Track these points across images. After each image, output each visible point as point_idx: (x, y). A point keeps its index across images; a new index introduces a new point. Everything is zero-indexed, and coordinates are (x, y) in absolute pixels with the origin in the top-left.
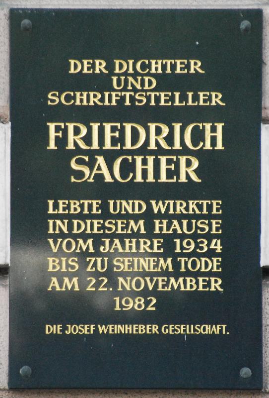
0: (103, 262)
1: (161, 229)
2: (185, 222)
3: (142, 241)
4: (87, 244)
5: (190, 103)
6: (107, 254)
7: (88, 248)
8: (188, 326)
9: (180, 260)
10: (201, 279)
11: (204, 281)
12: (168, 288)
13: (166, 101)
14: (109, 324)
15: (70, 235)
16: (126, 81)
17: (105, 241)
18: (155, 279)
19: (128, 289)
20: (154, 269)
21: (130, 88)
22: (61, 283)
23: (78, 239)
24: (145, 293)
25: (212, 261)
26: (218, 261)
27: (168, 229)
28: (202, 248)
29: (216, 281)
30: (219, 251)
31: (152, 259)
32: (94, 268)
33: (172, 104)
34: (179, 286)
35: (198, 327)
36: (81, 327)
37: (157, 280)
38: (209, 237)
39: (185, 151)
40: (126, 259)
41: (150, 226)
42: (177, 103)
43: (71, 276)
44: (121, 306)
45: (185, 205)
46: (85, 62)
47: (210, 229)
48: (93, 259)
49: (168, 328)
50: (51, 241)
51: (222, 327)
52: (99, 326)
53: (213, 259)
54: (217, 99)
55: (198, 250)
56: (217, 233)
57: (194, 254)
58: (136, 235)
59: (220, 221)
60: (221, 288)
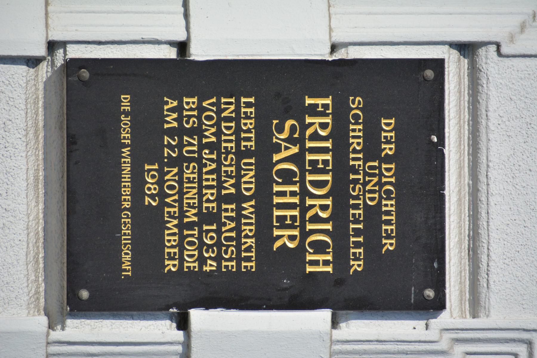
0: (193, 152)
1: (226, 210)
2: (233, 234)
3: (214, 191)
4: (211, 136)
5: (352, 239)
6: (201, 157)
7: (207, 137)
8: (130, 237)
9: (195, 230)
10: (176, 250)
11: (175, 253)
12: (167, 217)
13: (354, 215)
14: (131, 159)
15: (220, 120)
16: (374, 175)
17: (214, 154)
18: (177, 205)
19: (166, 178)
20: (187, 203)
21: (367, 179)
22: (171, 110)
23: (215, 127)
24: (162, 195)
25: (194, 262)
26: (194, 267)
27: (226, 217)
28: (207, 251)
29: (174, 266)
30: (205, 269)
31: (196, 201)
32: (186, 143)
33: (352, 221)
34: (169, 229)
35: (129, 247)
36: (128, 131)
37: (175, 207)
38: (218, 259)
39: (305, 234)
40: (196, 176)
41: (229, 199)
42: (352, 226)
43: (179, 120)
44: (149, 171)
45: (250, 234)
46: (393, 134)
47: (227, 260)
48: (196, 143)
49: (128, 218)
50: (214, 100)
51: (128, 271)
52: (129, 149)
53: (197, 262)
54: (357, 266)
55: (205, 248)
56: (223, 266)
57: (202, 244)
58: (220, 186)
59: (234, 270)
60: (168, 271)
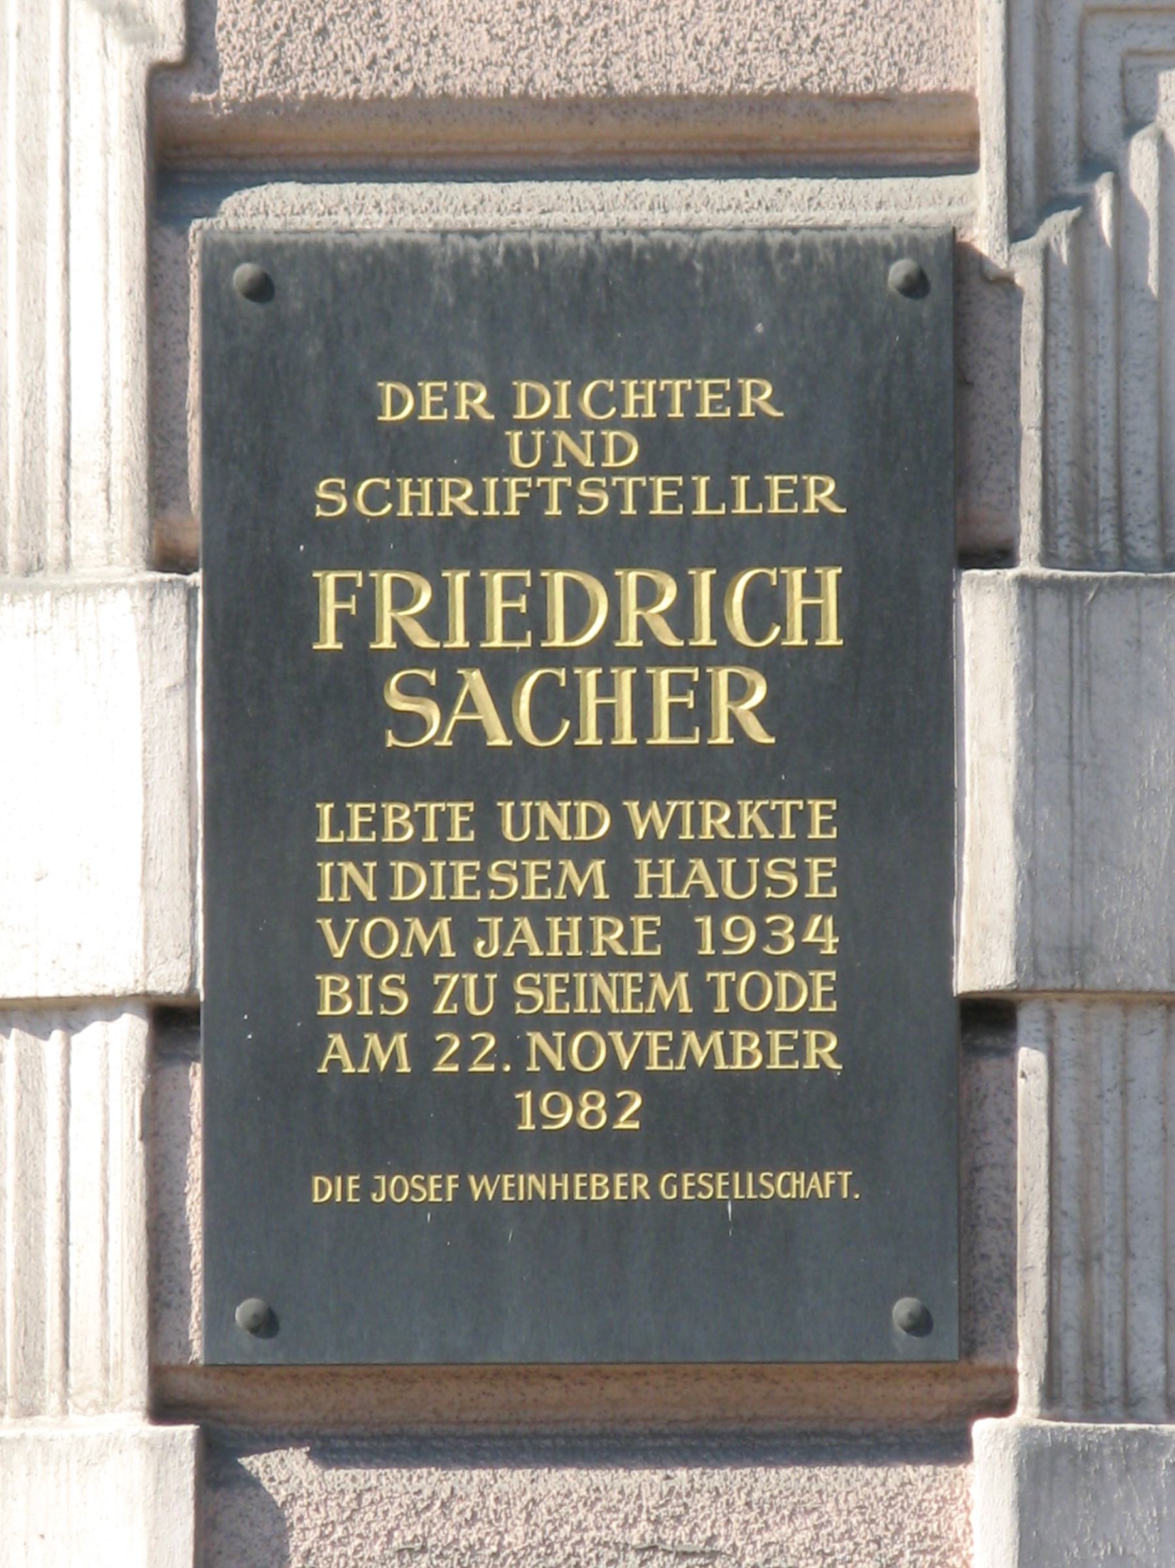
0: (481, 985)
1: (655, 885)
3: (599, 922)
7: (437, 945)
10: (776, 1035)
11: (785, 1040)
15: (385, 906)
19: (559, 1067)
21: (560, 464)
22: (356, 1049)
25: (810, 982)
26: (825, 981)
27: (677, 886)
29: (821, 1042)
31: (629, 977)
34: (711, 1057)
35: (766, 1178)
37: (645, 1040)
43: (386, 1028)
44: (538, 1117)
46: (427, 387)
47: (804, 884)
49: (678, 1181)
50: (326, 924)
51: (838, 1179)
57: (755, 958)
58: (584, 906)
59: (833, 862)
